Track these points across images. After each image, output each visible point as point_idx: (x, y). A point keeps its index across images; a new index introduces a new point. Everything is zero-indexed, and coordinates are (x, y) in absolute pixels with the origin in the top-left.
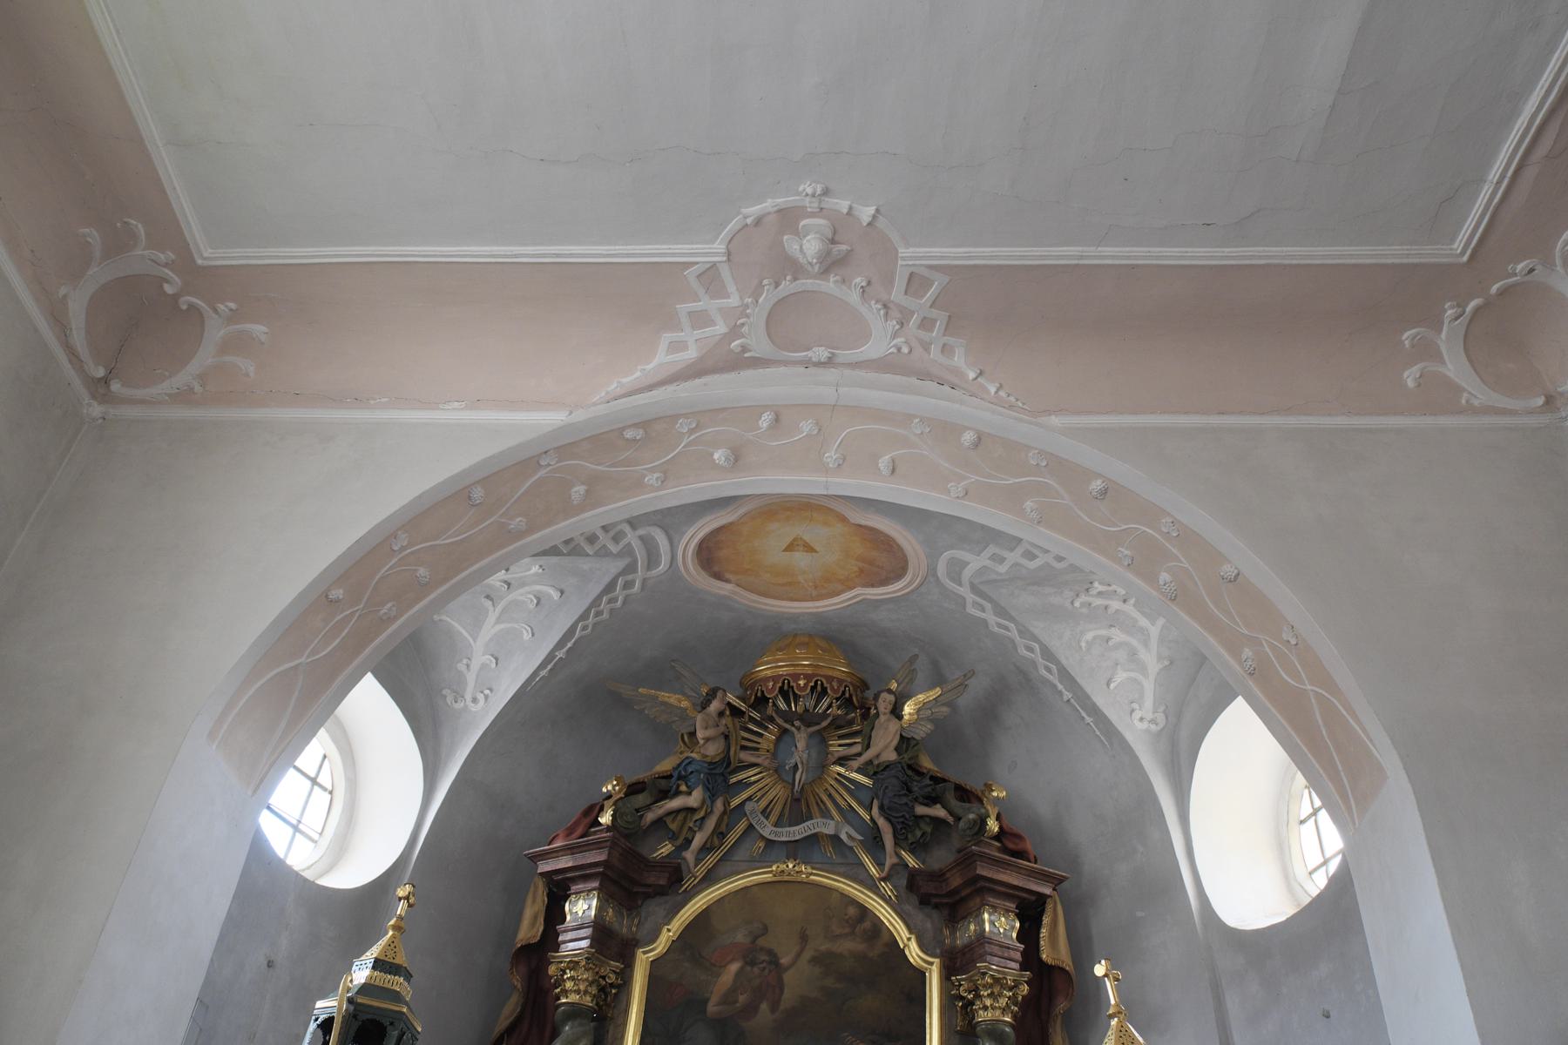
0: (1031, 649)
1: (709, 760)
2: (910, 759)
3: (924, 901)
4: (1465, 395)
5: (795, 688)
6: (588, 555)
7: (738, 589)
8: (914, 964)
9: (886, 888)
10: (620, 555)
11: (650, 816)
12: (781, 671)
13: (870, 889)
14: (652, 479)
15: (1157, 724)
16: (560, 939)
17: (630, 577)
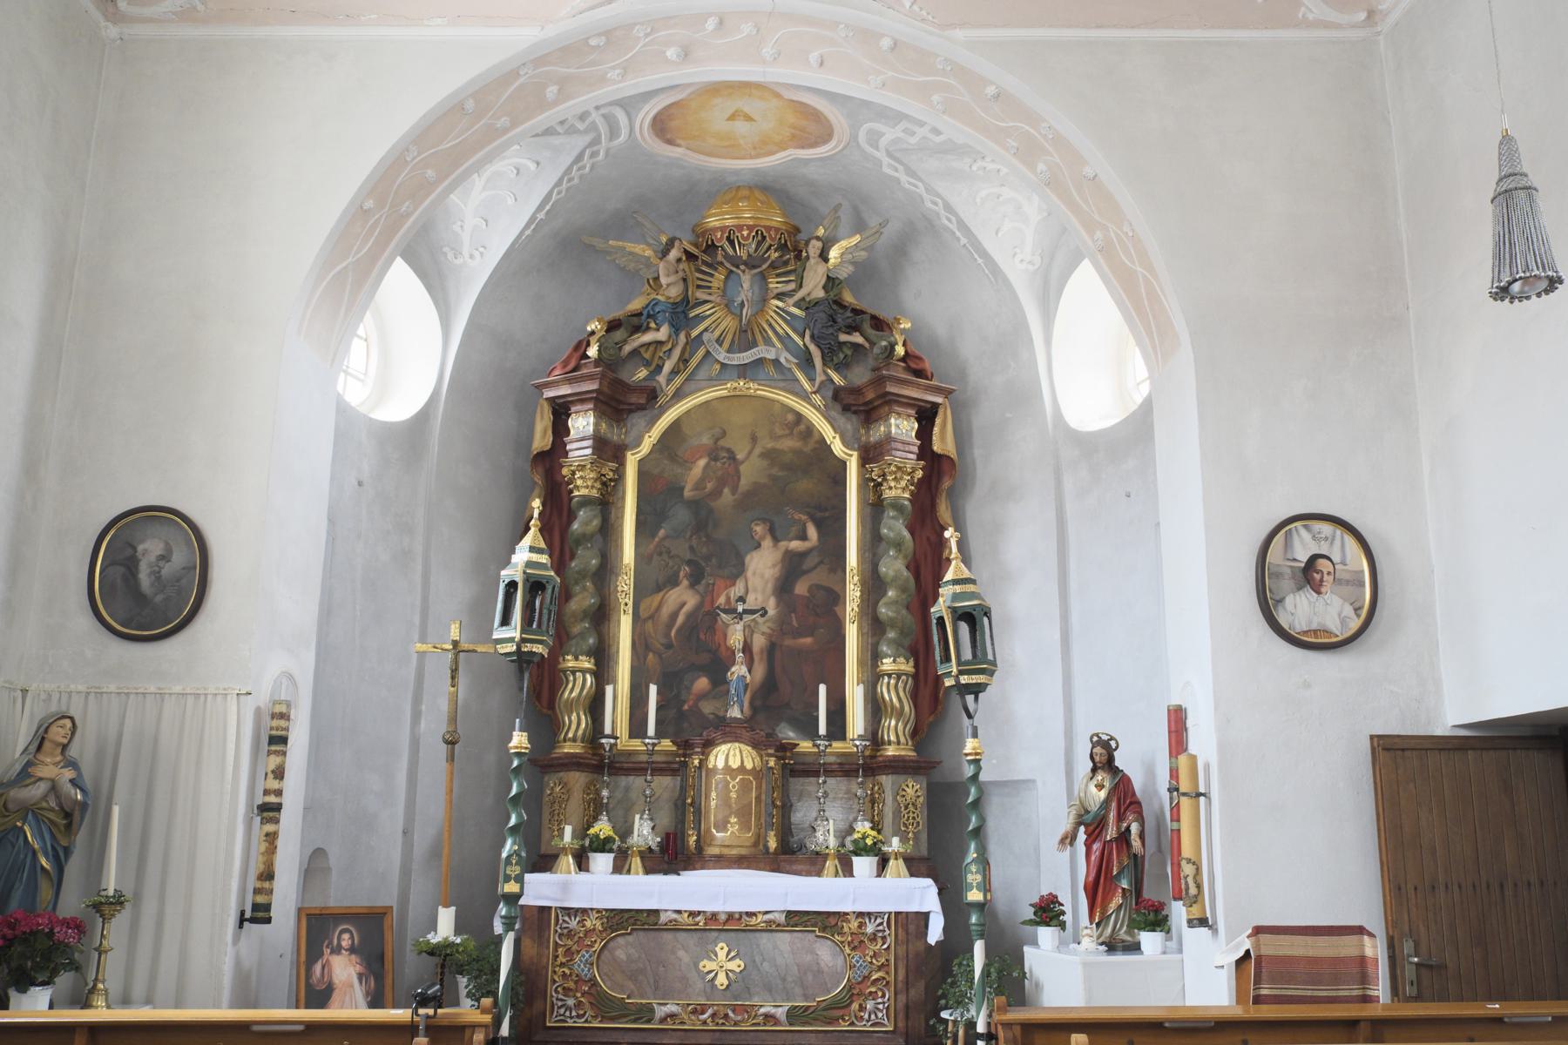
0: (935, 204)
1: (672, 301)
2: (835, 296)
3: (846, 409)
4: (1303, 9)
5: (740, 238)
6: (559, 134)
7: (689, 152)
8: (836, 453)
9: (817, 399)
10: (586, 131)
11: (627, 348)
12: (728, 223)
13: (804, 401)
14: (612, 75)
15: (1033, 265)
16: (568, 447)
17: (595, 148)
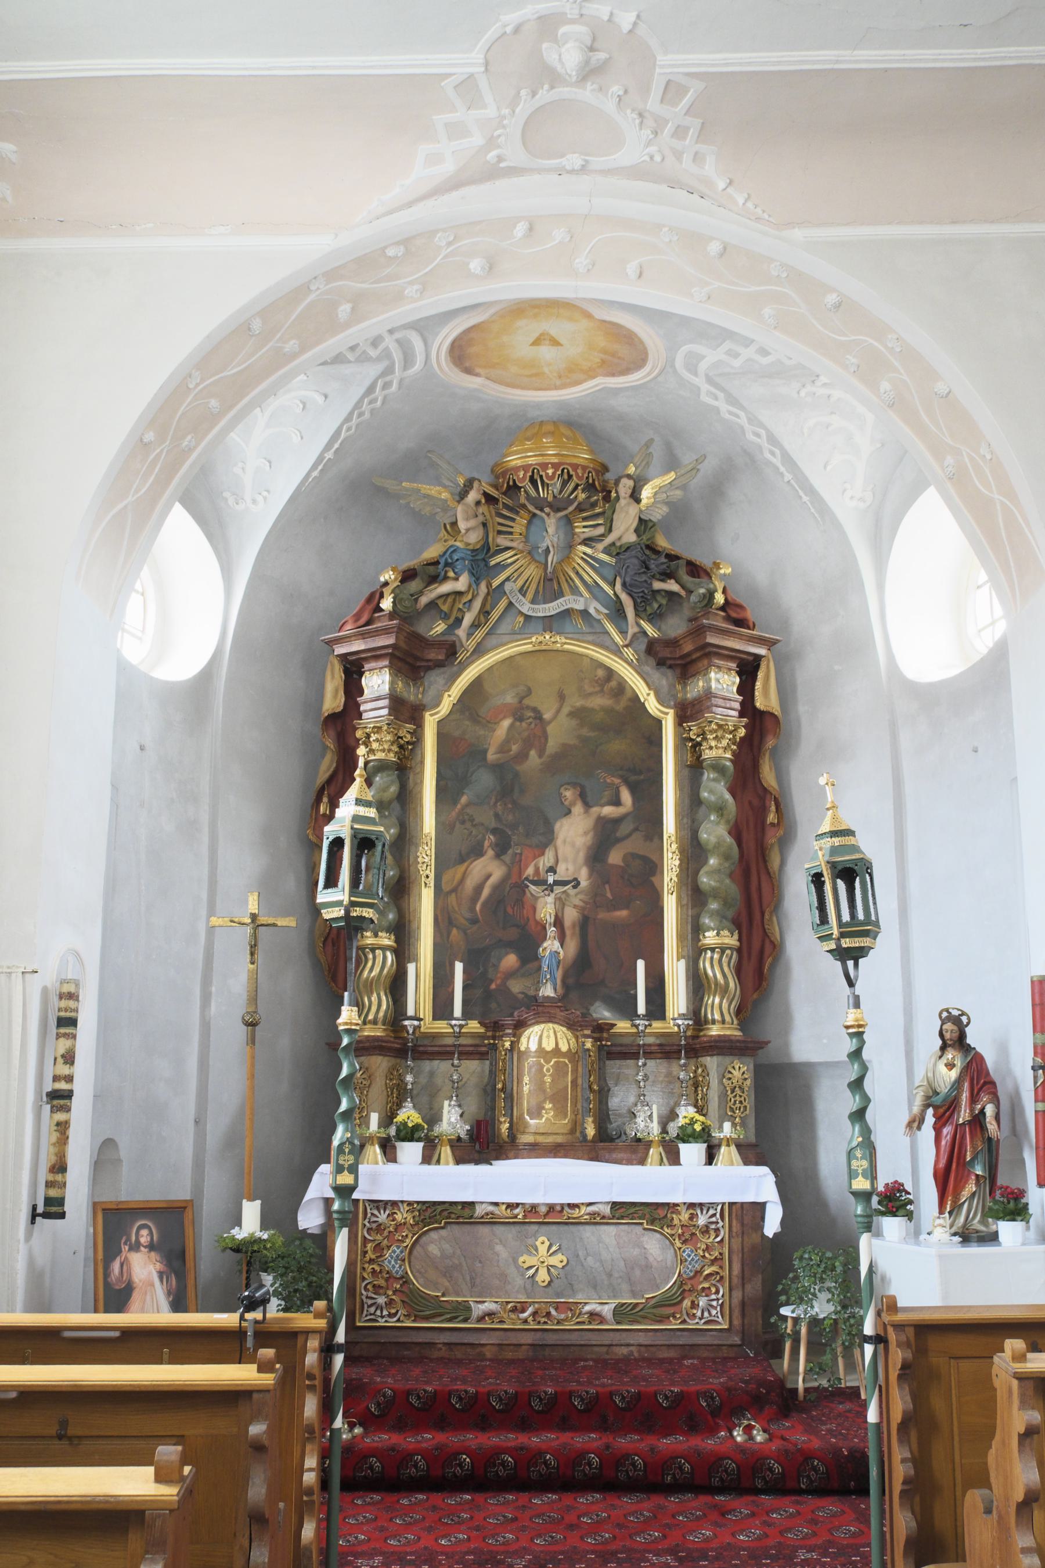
0: (758, 435)
1: (471, 547)
3: (661, 663)
6: (350, 362)
7: (488, 382)
8: (653, 714)
9: (629, 653)
10: (378, 359)
11: (424, 600)
12: (532, 461)
13: (615, 654)
14: (411, 291)
16: (362, 708)
17: (388, 379)
